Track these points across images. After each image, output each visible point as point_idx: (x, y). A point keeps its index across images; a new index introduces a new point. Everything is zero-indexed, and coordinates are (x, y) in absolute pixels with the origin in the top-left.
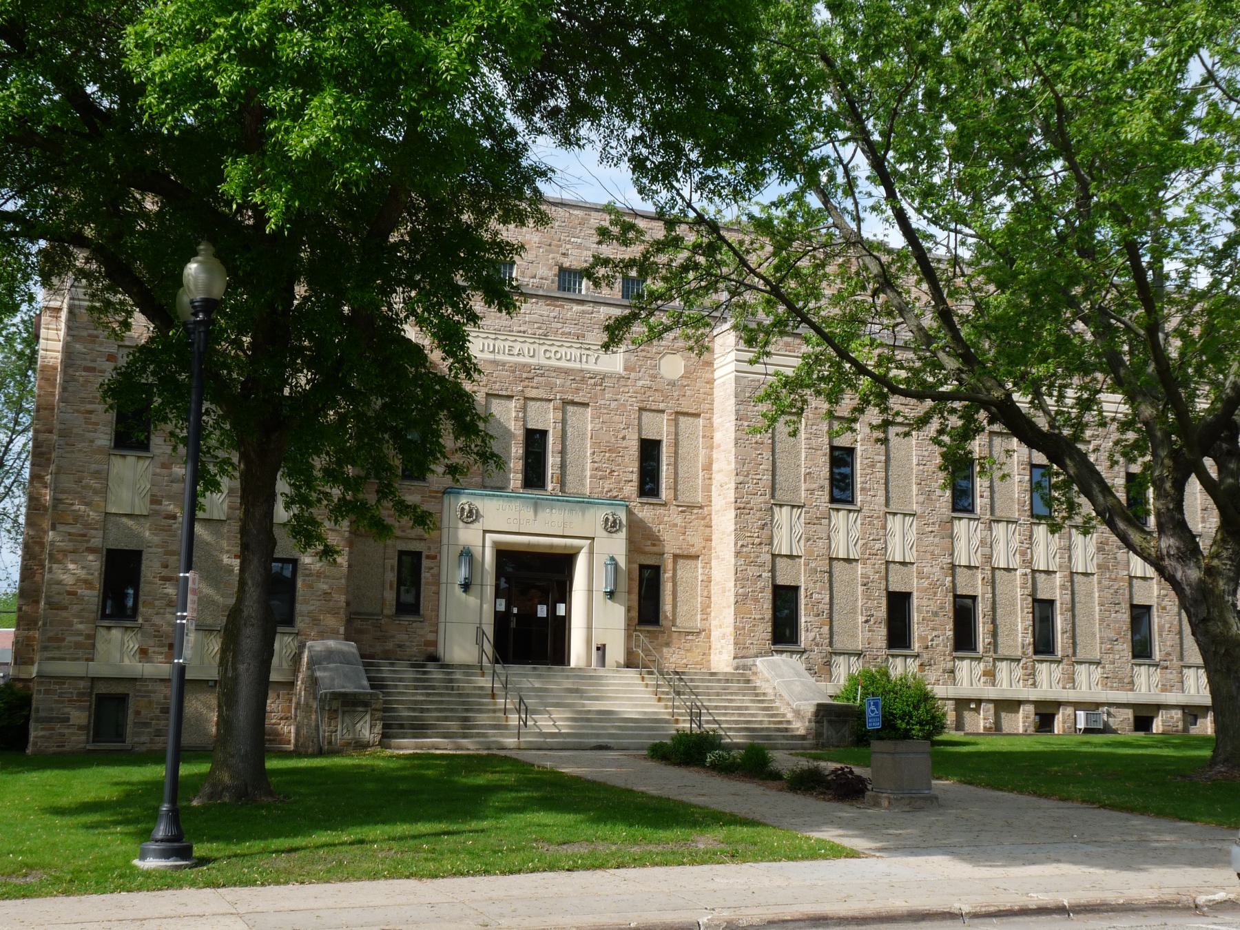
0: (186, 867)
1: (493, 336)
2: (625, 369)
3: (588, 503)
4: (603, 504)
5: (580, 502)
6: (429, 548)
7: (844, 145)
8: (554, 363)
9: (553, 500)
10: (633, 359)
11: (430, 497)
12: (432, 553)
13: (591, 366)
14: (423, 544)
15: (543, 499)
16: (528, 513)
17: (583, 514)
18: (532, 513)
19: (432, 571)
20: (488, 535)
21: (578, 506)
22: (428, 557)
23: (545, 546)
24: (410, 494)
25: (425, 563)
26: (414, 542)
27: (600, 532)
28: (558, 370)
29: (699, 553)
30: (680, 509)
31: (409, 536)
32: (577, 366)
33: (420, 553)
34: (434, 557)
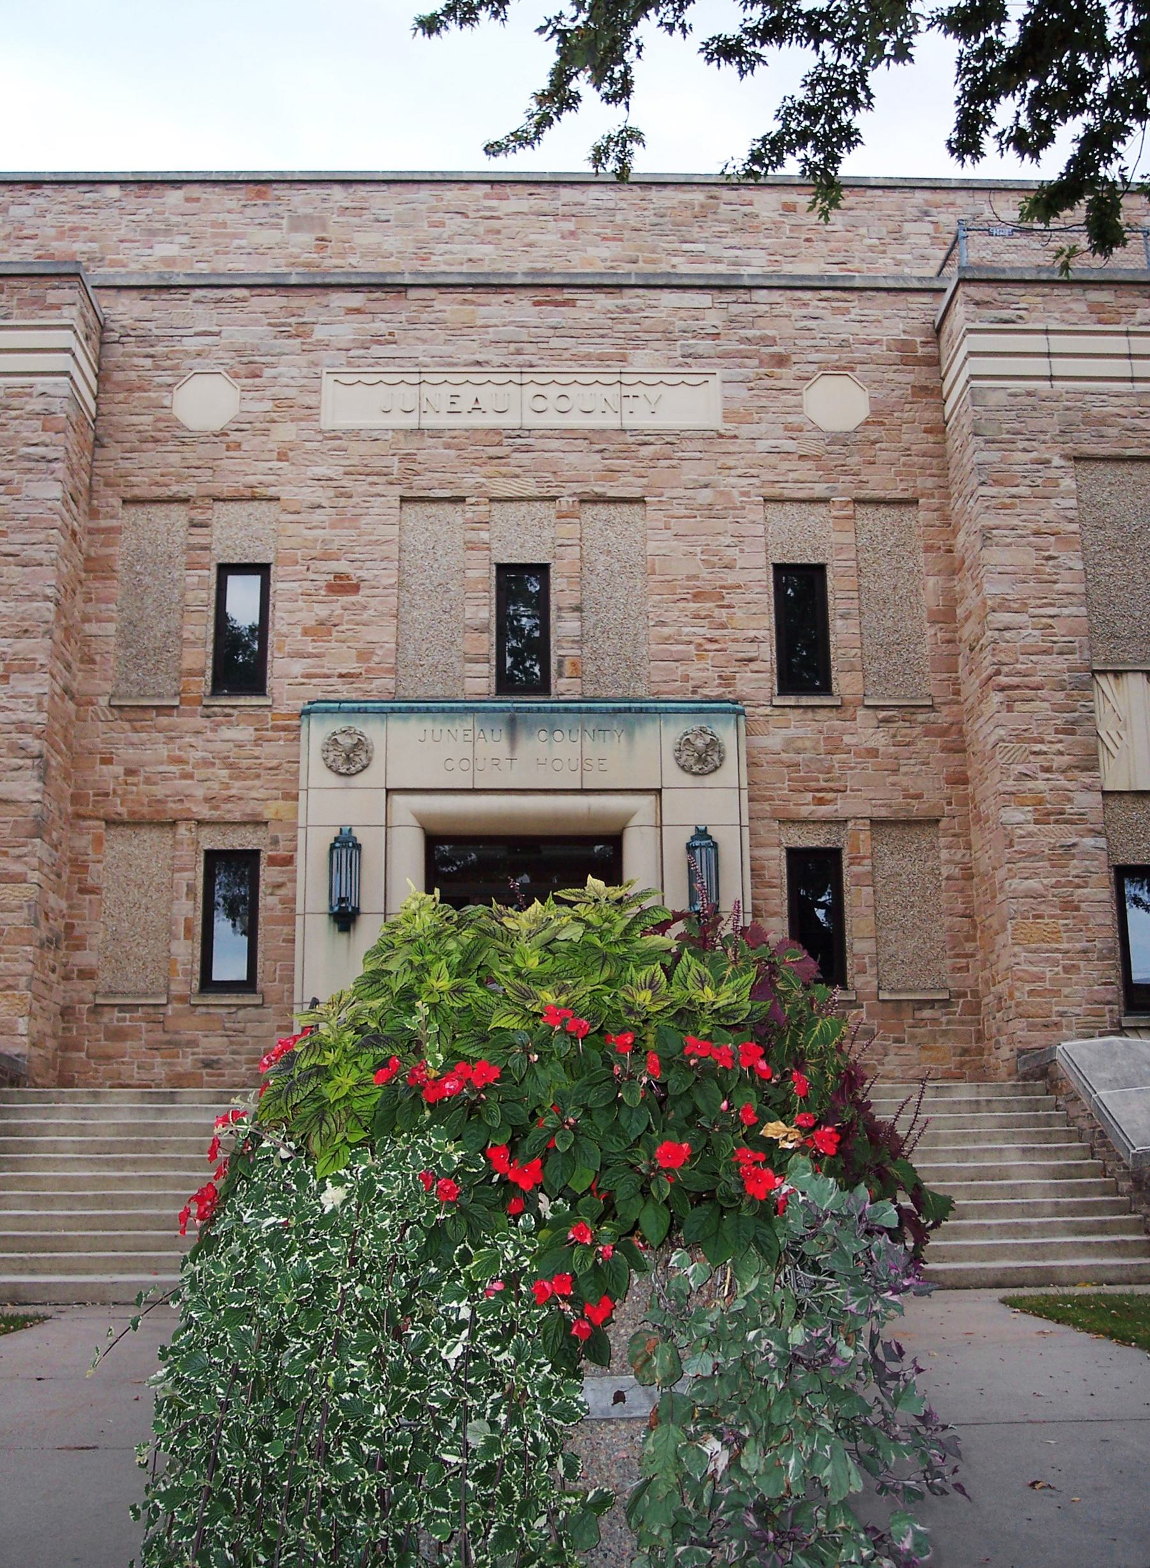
0: (94, 370)
1: (415, 379)
2: (726, 417)
3: (640, 711)
4: (677, 711)
5: (620, 711)
6: (275, 841)
7: (782, 165)
8: (552, 420)
9: (552, 710)
10: (741, 392)
11: (275, 728)
12: (282, 852)
13: (641, 420)
14: (261, 832)
15: (529, 710)
16: (495, 744)
17: (630, 736)
18: (504, 744)
19: (282, 892)
20: (397, 799)
21: (615, 723)
22: (273, 861)
23: (540, 819)
24: (231, 725)
25: (268, 874)
26: (242, 831)
27: (673, 776)
28: (569, 434)
29: (937, 813)
30: (882, 714)
31: (229, 817)
32: (612, 422)
33: (256, 853)
34: (289, 861)
